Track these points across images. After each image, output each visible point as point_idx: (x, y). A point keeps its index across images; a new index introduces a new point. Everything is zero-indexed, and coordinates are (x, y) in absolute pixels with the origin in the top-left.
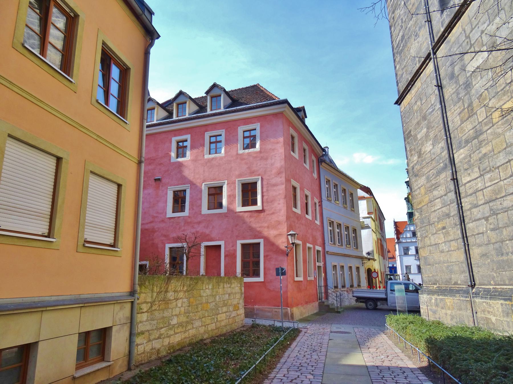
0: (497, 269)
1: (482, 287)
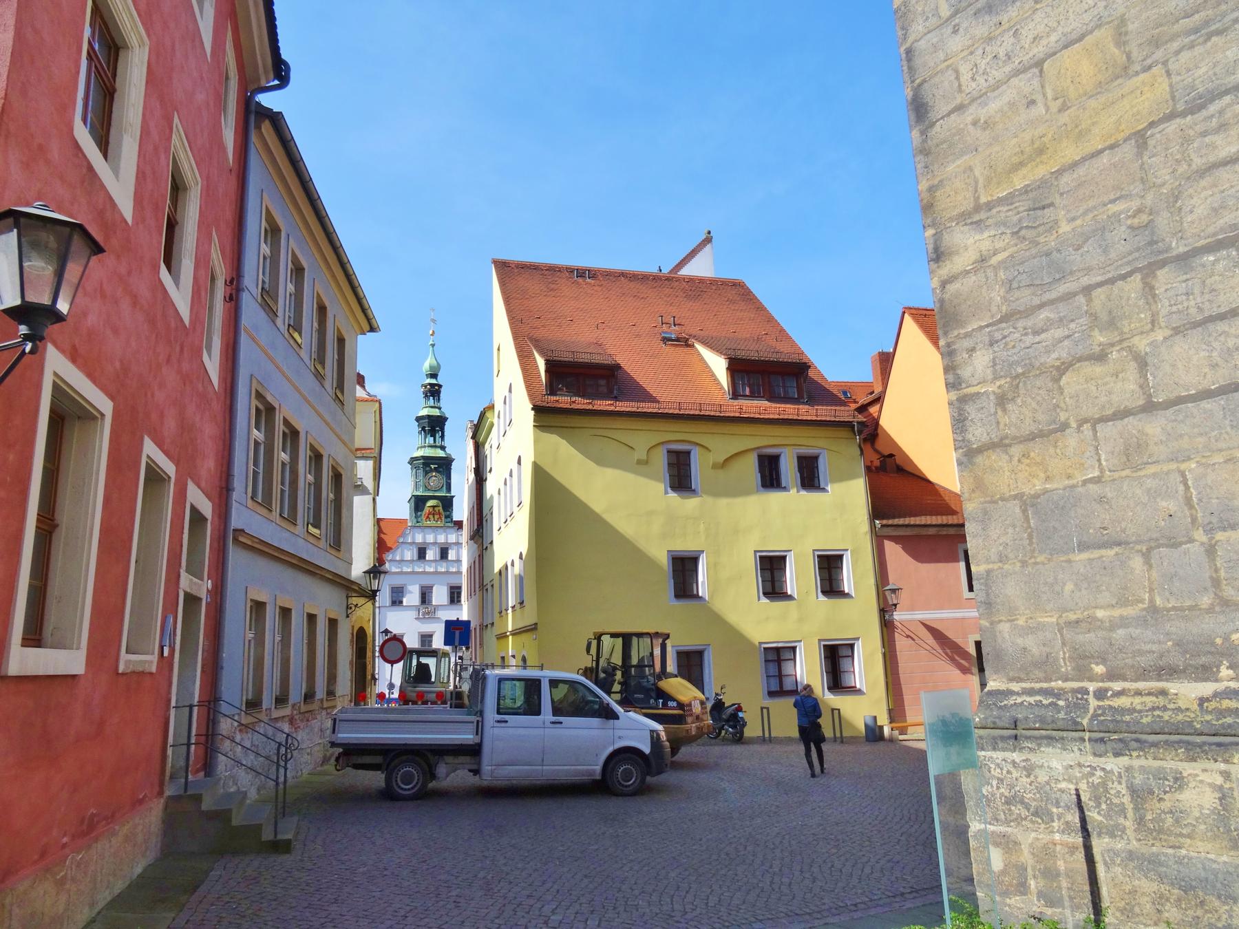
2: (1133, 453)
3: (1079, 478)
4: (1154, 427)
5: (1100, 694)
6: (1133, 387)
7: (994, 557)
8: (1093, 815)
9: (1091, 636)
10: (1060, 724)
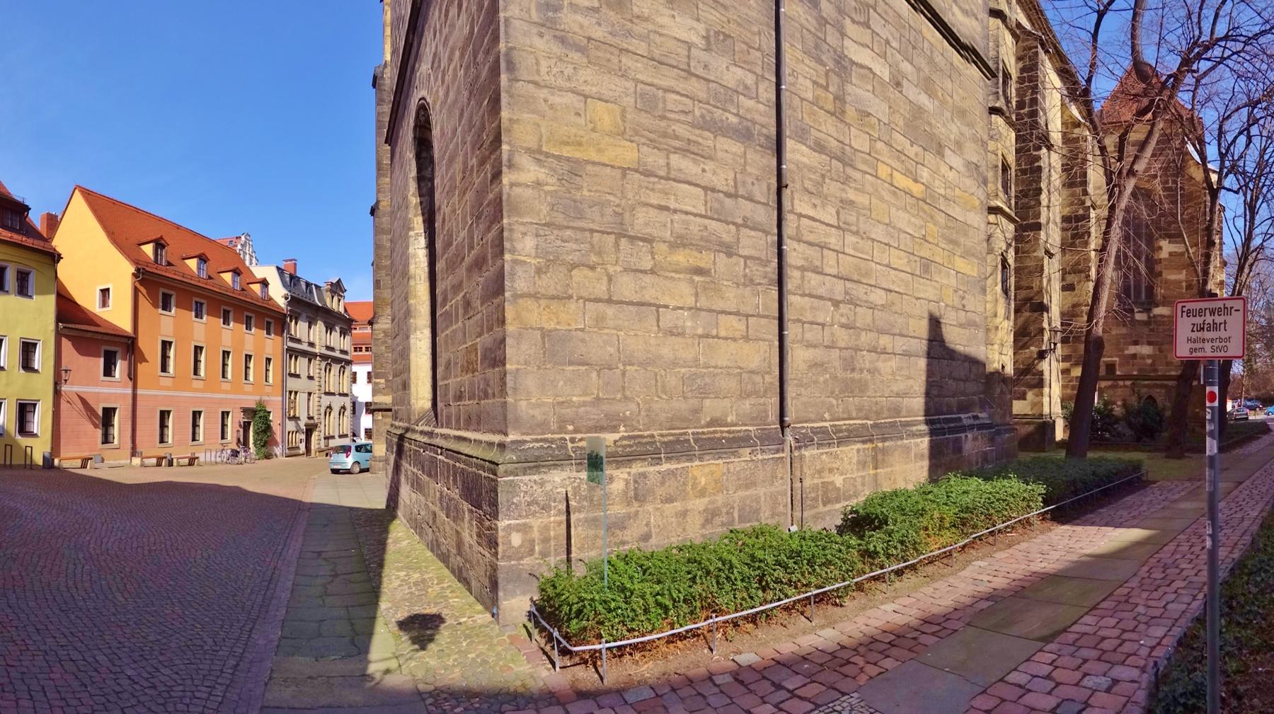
0: (842, 391)
1: (805, 425)
2: (600, 320)
3: (574, 327)
4: (610, 311)
5: (573, 440)
6: (604, 288)
7: (522, 361)
8: (572, 503)
9: (568, 410)
10: (561, 457)
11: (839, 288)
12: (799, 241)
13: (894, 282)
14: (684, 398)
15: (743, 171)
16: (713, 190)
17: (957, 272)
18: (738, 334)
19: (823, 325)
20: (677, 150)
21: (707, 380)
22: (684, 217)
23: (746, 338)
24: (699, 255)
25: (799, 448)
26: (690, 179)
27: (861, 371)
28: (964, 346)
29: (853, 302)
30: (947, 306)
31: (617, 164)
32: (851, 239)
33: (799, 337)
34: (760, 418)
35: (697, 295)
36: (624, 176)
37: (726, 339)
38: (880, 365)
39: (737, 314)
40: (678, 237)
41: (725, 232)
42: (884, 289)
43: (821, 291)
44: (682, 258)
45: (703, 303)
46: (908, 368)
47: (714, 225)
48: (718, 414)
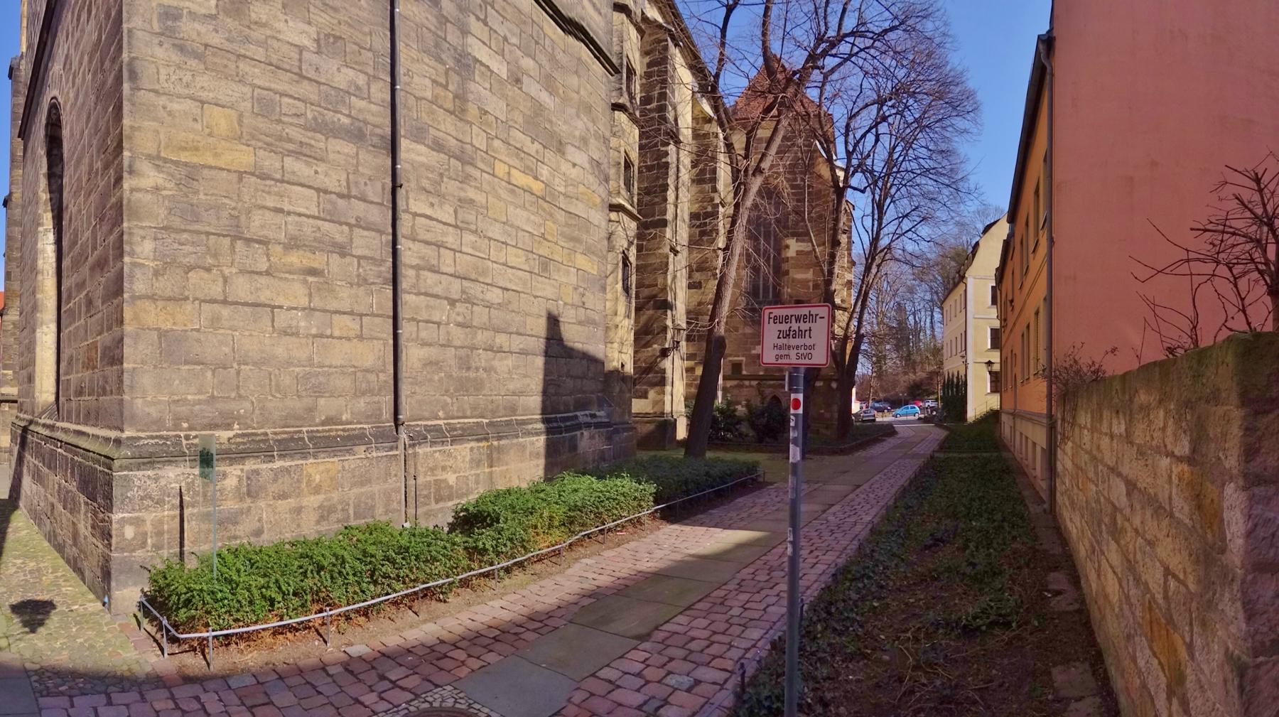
3: (190, 327)
11: (455, 287)
12: (414, 240)
13: (511, 281)
14: (298, 396)
15: (356, 171)
16: (326, 192)
17: (578, 270)
18: (352, 334)
19: (439, 324)
20: (290, 153)
21: (321, 379)
22: (297, 218)
23: (360, 337)
24: (312, 256)
25: (414, 445)
26: (302, 181)
27: (477, 369)
28: (583, 343)
29: (469, 300)
30: (565, 304)
31: (233, 168)
32: (469, 238)
33: (414, 336)
34: (374, 416)
35: (310, 295)
36: (240, 180)
37: (340, 338)
38: (496, 363)
39: (351, 313)
40: (291, 239)
41: (338, 233)
42: (501, 288)
43: (438, 290)
44: (296, 259)
45: (317, 302)
46: (525, 366)
47: (326, 226)
48: (332, 413)
